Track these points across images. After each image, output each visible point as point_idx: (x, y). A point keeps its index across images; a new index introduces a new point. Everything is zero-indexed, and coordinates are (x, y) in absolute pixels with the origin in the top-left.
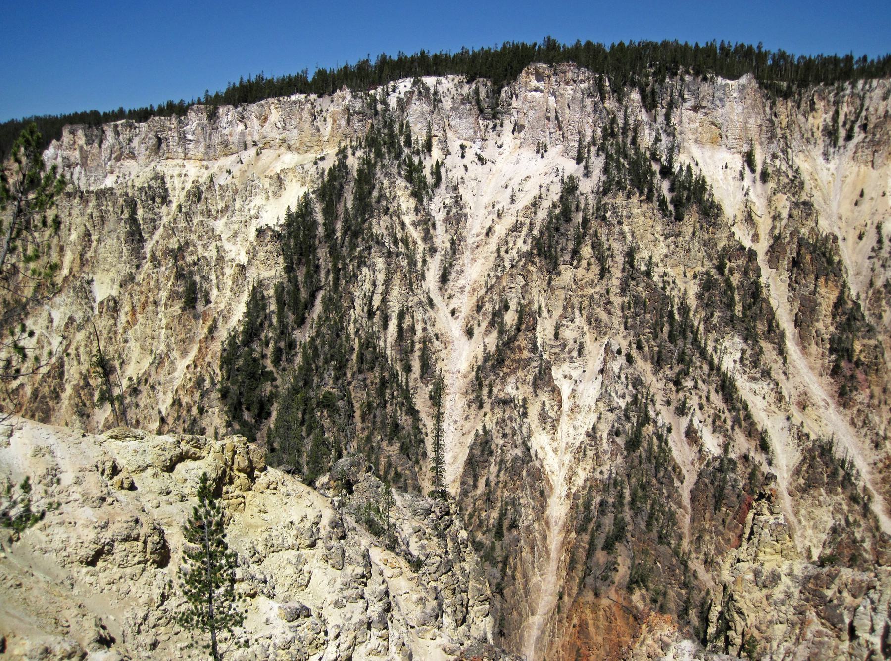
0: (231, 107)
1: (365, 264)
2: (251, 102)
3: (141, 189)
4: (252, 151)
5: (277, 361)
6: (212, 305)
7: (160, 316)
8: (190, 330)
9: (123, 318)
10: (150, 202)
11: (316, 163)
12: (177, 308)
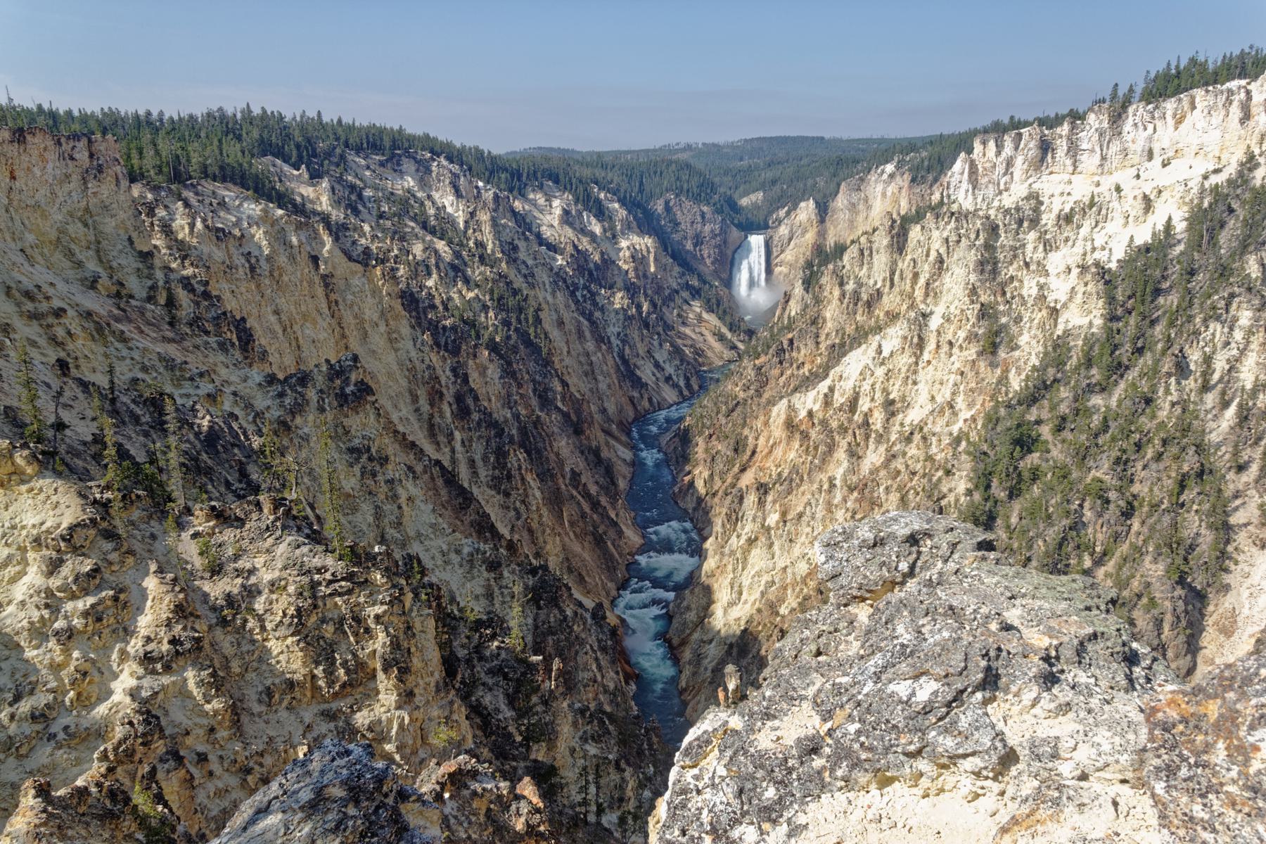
0: (1142, 105)
1: (1218, 318)
2: (1169, 97)
3: (1007, 211)
4: (1157, 161)
5: (1059, 429)
6: (1017, 353)
7: (952, 359)
8: (983, 380)
9: (926, 356)
10: (1015, 226)
11: (1206, 177)
12: (972, 353)
